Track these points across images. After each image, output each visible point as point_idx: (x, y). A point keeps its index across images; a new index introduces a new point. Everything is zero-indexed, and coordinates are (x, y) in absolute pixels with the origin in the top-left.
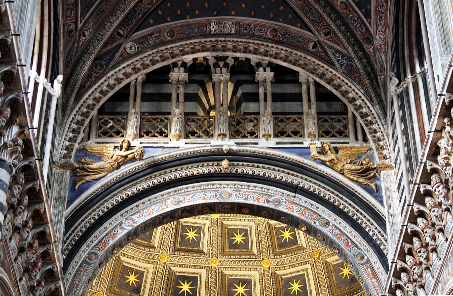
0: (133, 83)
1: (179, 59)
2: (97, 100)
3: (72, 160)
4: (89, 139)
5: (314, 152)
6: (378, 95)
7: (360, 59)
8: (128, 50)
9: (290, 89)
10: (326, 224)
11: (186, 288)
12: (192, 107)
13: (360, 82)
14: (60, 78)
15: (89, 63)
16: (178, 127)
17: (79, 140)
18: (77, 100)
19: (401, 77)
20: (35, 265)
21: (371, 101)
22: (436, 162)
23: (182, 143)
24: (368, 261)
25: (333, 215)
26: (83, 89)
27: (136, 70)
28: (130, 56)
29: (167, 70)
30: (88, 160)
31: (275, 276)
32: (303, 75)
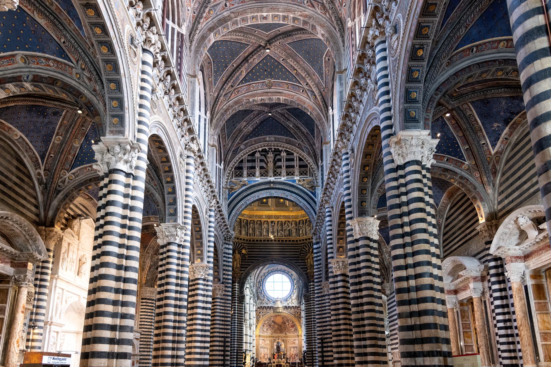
1: (257, 150)
5: (297, 182)
6: (317, 162)
9: (291, 157)
10: (301, 202)
13: (312, 157)
14: (223, 162)
18: (228, 166)
23: (259, 179)
26: (230, 162)
27: (244, 154)
28: (243, 150)
29: (255, 153)
32: (295, 154)
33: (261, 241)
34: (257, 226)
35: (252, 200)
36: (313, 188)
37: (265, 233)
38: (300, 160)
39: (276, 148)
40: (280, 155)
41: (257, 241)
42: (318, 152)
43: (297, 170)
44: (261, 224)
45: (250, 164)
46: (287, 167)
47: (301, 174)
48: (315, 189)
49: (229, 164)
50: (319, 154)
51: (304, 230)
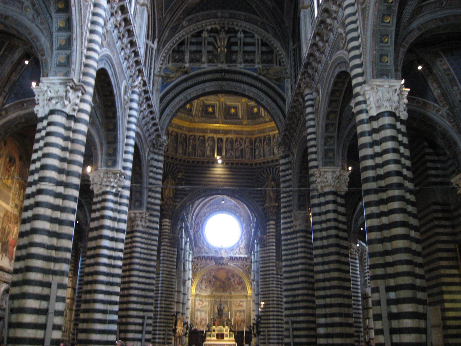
0: (186, 39)
2: (171, 47)
4: (168, 63)
10: (263, 100)
11: (210, 110)
12: (210, 48)
13: (279, 40)
14: (157, 40)
17: (165, 64)
18: (163, 47)
20: (149, 122)
21: (283, 48)
22: (300, 90)
23: (205, 65)
24: (278, 115)
25: (266, 96)
28: (185, 27)
29: (201, 32)
31: (247, 105)
32: (256, 36)
33: (203, 162)
34: (198, 143)
35: (195, 94)
36: (280, 80)
37: (209, 153)
40: (236, 37)
41: (198, 162)
44: (204, 141)
45: (194, 48)
47: (263, 61)
49: (164, 45)
50: (290, 35)
51: (262, 151)
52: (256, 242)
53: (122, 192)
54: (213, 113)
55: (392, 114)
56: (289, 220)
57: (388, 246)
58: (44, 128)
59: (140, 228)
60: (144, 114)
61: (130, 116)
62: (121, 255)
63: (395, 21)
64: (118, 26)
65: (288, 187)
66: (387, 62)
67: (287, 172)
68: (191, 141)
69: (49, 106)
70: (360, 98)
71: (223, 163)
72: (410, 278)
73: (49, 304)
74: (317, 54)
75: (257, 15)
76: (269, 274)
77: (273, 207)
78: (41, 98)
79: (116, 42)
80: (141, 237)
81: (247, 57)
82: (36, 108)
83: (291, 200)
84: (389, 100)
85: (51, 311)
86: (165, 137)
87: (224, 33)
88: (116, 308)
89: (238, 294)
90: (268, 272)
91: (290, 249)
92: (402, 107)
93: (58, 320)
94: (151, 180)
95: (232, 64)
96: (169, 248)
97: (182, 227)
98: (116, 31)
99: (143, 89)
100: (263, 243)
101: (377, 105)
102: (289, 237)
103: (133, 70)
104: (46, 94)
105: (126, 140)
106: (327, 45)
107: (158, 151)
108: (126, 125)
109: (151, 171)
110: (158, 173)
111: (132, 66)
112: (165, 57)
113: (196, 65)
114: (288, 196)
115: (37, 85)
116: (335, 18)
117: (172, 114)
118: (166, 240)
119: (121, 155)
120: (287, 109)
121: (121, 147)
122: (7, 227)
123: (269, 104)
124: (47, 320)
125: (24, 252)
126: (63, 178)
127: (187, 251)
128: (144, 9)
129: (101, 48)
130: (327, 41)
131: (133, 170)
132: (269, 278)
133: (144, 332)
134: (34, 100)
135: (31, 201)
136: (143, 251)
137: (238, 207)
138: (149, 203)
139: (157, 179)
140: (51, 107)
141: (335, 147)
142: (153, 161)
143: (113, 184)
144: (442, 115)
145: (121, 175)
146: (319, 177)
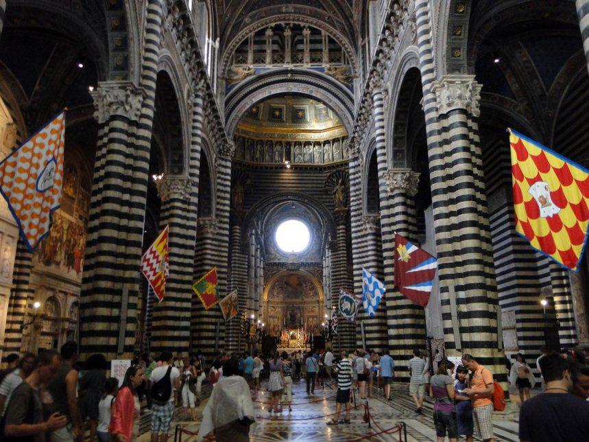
2: (234, 46)
3: (226, 75)
4: (232, 64)
7: (348, 26)
8: (247, 22)
9: (317, 37)
10: (331, 101)
11: (277, 113)
12: (276, 47)
13: (348, 37)
15: (230, 30)
16: (270, 58)
18: (226, 47)
19: (363, 38)
20: (214, 127)
21: (351, 45)
23: (270, 66)
26: (228, 41)
27: (250, 31)
29: (264, 30)
30: (233, 75)
32: (323, 32)
33: (271, 168)
36: (349, 80)
37: (277, 158)
38: (331, 41)
39: (297, 23)
40: (301, 34)
42: (358, 27)
43: (325, 57)
46: (311, 51)
47: (331, 60)
48: (352, 81)
50: (359, 30)
51: (331, 155)
52: (327, 247)
53: (190, 199)
54: (280, 116)
55: (463, 111)
56: (359, 223)
57: (458, 246)
58: (106, 135)
59: (210, 235)
60: (209, 119)
61: (195, 121)
62: (191, 261)
63: (469, 11)
64: (177, 24)
65: (358, 190)
66: (459, 56)
67: (357, 175)
68: (259, 147)
69: (109, 112)
70: (430, 96)
71: (291, 168)
72: (479, 277)
73: (120, 311)
74: (386, 50)
75: (325, 9)
76: (340, 279)
77: (344, 211)
78: (100, 105)
79: (175, 41)
80: (211, 244)
81: (313, 56)
82: (96, 114)
83: (360, 204)
84: (460, 97)
85: (123, 317)
86: (232, 143)
87: (289, 30)
88: (188, 314)
89: (309, 300)
90: (339, 277)
91: (360, 253)
92: (474, 104)
93: (131, 327)
94: (219, 187)
95: (298, 64)
96: (240, 255)
97: (252, 234)
98: (174, 31)
99: (207, 92)
100: (334, 247)
101: (448, 102)
102: (359, 240)
103: (195, 73)
104: (105, 100)
105: (192, 147)
106: (397, 39)
107: (224, 157)
108: (191, 131)
109: (219, 178)
110: (226, 180)
111: (194, 68)
112: (228, 58)
113: (261, 66)
114: (358, 200)
115: (95, 89)
116: (406, 10)
117: (238, 119)
118: (237, 247)
119: (187, 162)
120: (355, 110)
121: (187, 153)
122: (72, 240)
123: (337, 105)
124: (119, 327)
125: (93, 261)
126: (128, 185)
127: (258, 258)
128: (202, 6)
129: (160, 49)
130: (397, 36)
131: (200, 177)
132: (341, 282)
133: (217, 339)
134: (93, 106)
135: (98, 210)
136: (213, 258)
137: (308, 213)
138: (218, 209)
139: (226, 186)
140: (112, 113)
141: (404, 148)
142: (221, 167)
143: (180, 191)
144: (519, 112)
145: (188, 182)
146: (389, 179)
